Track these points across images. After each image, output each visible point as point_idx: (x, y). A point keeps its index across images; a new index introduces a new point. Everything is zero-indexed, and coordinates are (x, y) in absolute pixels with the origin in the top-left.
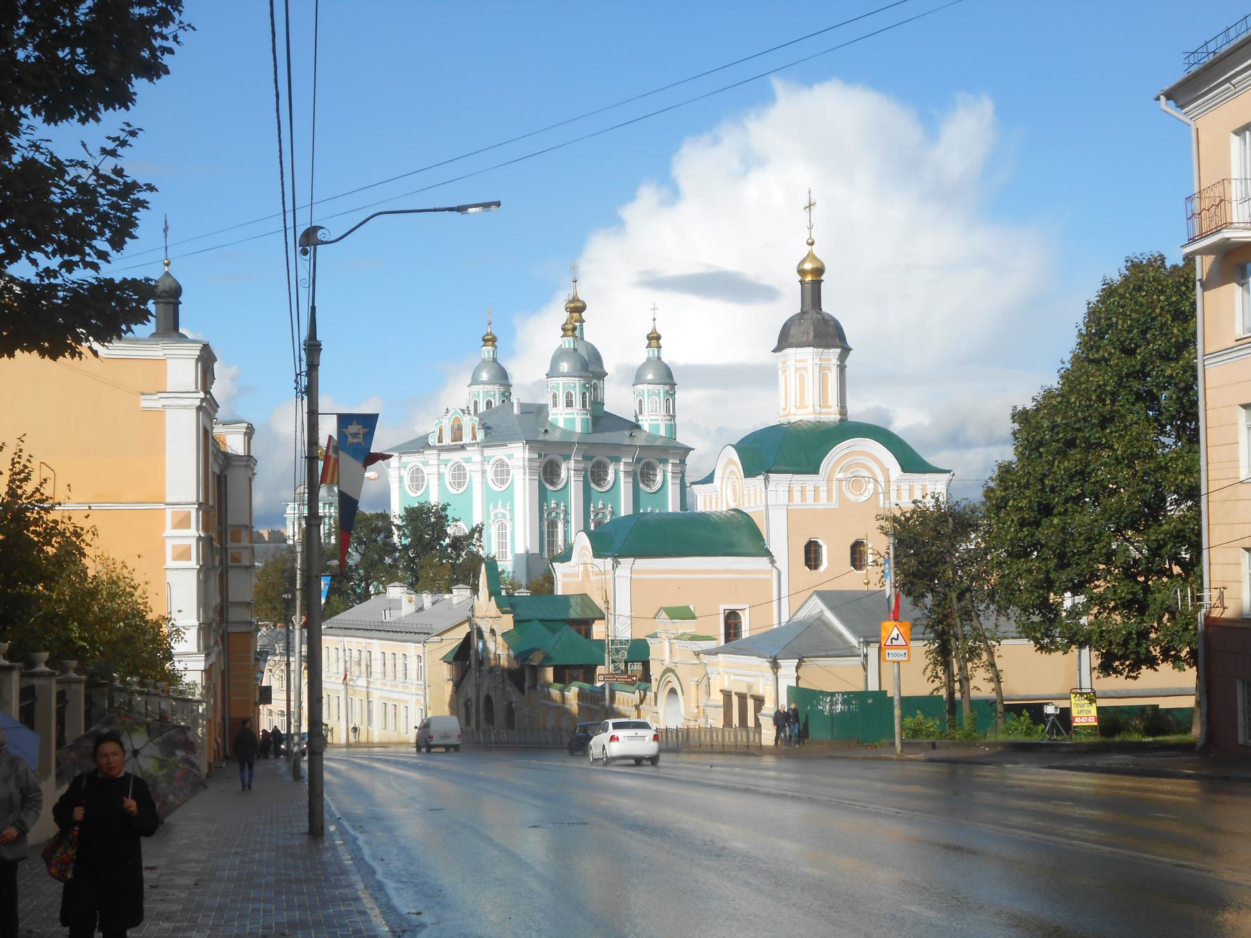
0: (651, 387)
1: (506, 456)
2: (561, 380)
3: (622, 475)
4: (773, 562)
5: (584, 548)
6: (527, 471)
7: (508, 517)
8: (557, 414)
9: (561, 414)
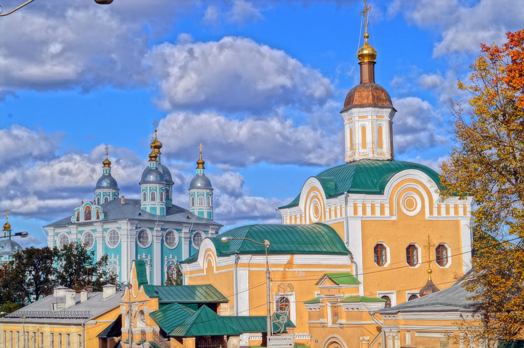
0: (199, 190)
1: (116, 228)
2: (149, 186)
3: (183, 239)
4: (352, 258)
5: (208, 250)
6: (129, 236)
7: (118, 263)
8: (146, 205)
9: (148, 205)
